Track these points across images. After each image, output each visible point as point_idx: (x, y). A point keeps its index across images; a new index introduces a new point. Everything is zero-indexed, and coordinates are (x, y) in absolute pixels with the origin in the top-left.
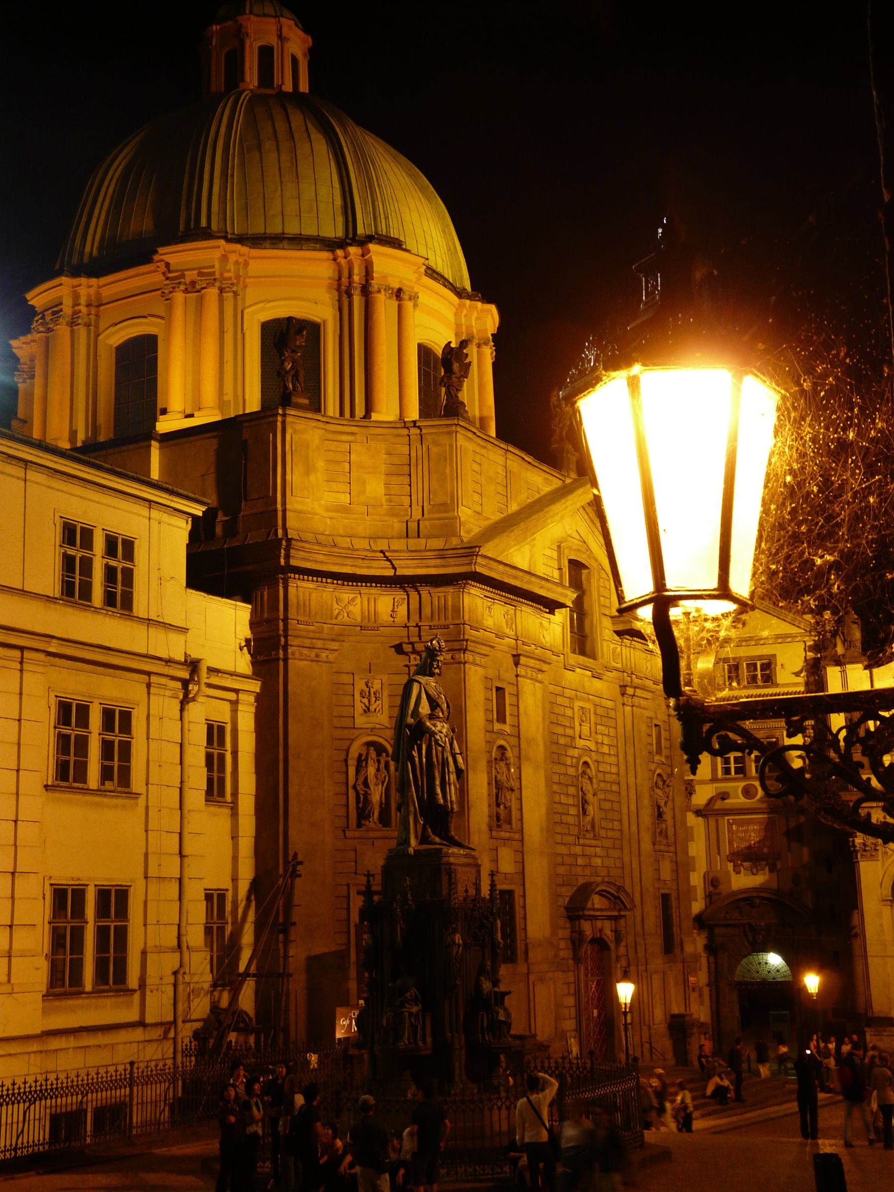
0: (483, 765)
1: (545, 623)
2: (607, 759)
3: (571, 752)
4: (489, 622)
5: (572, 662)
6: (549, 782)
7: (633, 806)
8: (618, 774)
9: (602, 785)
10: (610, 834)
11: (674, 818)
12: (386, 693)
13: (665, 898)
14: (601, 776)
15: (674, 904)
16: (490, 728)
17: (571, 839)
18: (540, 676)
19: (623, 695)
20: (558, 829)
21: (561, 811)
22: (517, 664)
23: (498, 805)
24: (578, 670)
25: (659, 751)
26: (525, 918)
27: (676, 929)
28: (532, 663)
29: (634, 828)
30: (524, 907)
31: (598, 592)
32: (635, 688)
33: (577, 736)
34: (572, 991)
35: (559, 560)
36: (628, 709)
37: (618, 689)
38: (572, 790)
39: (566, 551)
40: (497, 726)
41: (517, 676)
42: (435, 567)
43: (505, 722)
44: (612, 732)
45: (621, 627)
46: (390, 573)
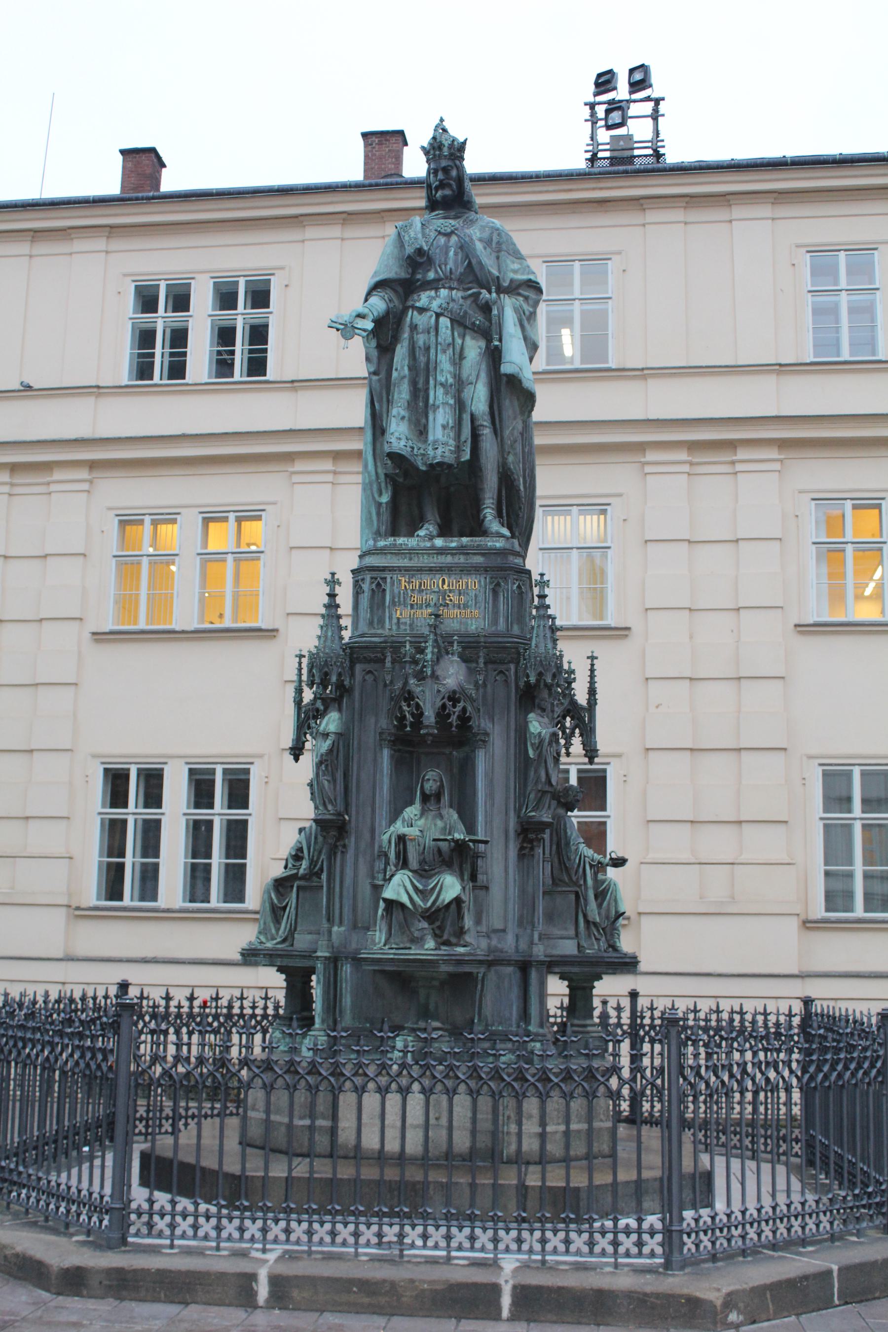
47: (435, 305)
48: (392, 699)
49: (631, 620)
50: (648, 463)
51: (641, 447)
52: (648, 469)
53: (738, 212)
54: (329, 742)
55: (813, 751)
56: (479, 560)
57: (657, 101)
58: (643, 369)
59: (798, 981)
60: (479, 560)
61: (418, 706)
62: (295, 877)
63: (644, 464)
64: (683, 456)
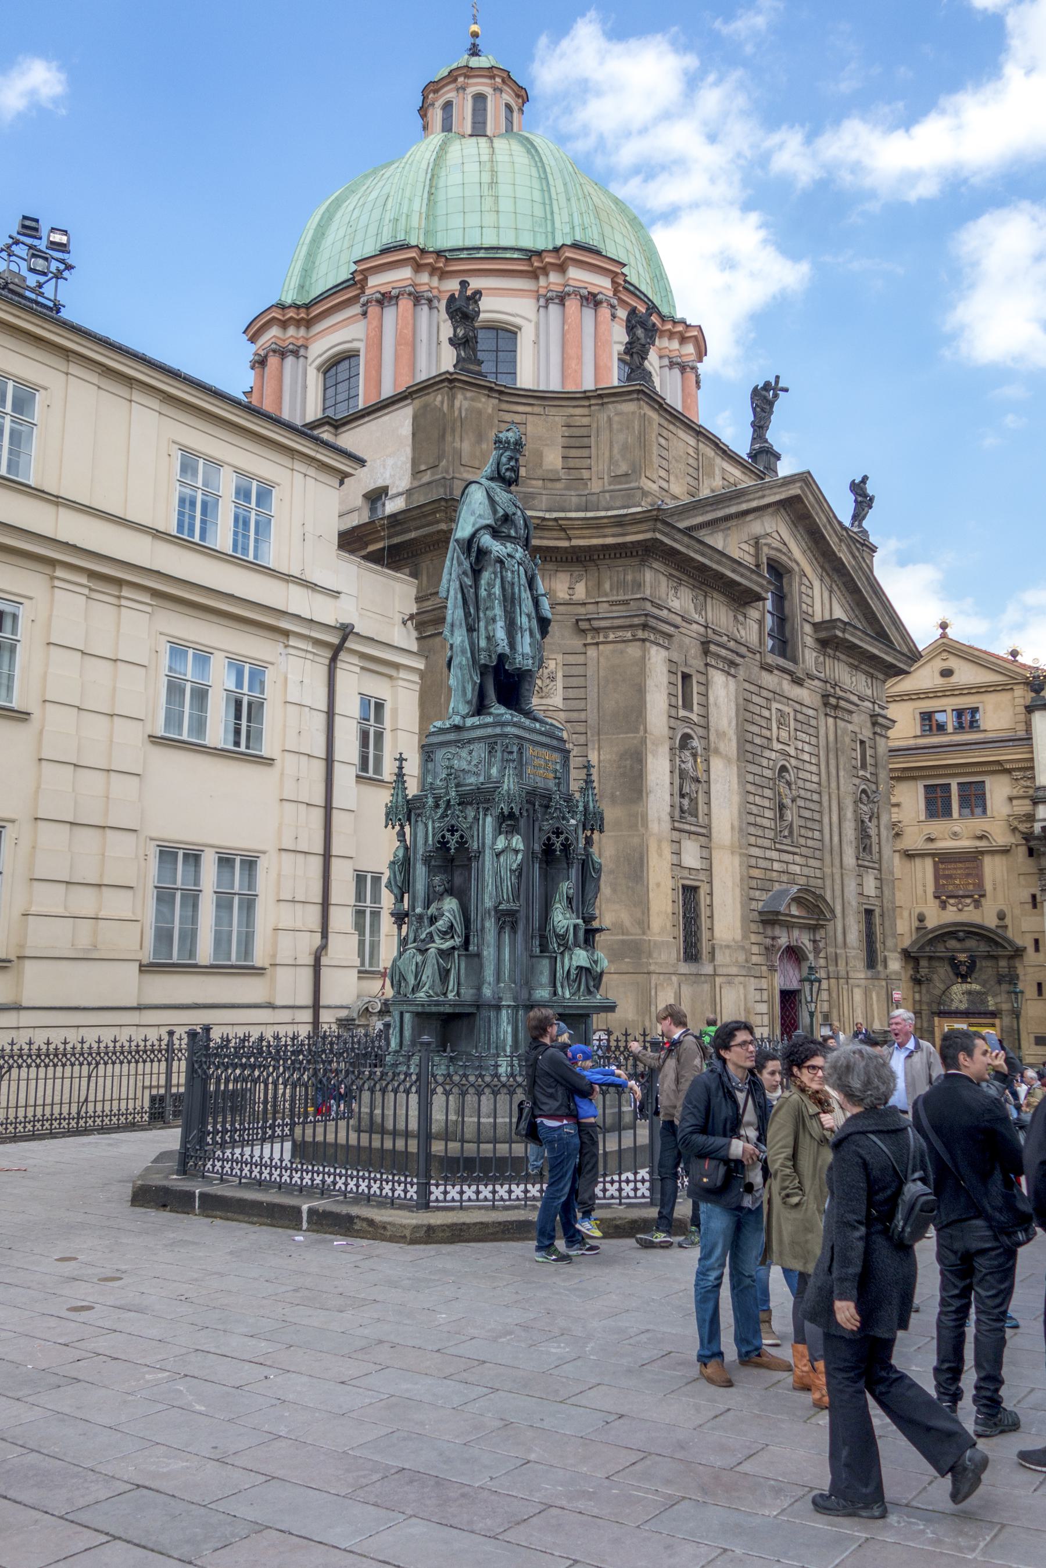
0: (664, 750)
1: (741, 618)
2: (807, 767)
3: (767, 753)
4: (675, 604)
5: (769, 661)
6: (742, 782)
7: (835, 818)
8: (819, 784)
9: (802, 793)
10: (810, 843)
11: (879, 835)
12: (560, 675)
13: (869, 913)
14: (800, 783)
15: (877, 920)
16: (673, 713)
17: (767, 843)
18: (733, 671)
19: (826, 704)
20: (752, 830)
21: (755, 812)
22: (706, 652)
23: (682, 796)
24: (776, 672)
25: (864, 766)
26: (711, 917)
27: (878, 945)
28: (723, 652)
29: (836, 839)
30: (711, 906)
31: (800, 598)
32: (839, 698)
33: (774, 737)
34: (765, 998)
35: (757, 556)
36: (831, 720)
37: (819, 698)
38: (768, 793)
39: (765, 550)
40: (682, 713)
41: (707, 665)
42: (613, 536)
43: (691, 710)
44: (814, 741)
45: (823, 635)
46: (565, 544)
47: (518, 555)
48: (540, 830)
49: (31, 705)
50: (58, 578)
51: (52, 563)
52: (57, 583)
53: (137, 396)
54: (520, 857)
55: (154, 835)
56: (555, 743)
57: (69, 267)
58: (57, 497)
59: (136, 1013)
60: (555, 743)
61: (567, 839)
62: (453, 948)
63: (53, 578)
64: (84, 580)
